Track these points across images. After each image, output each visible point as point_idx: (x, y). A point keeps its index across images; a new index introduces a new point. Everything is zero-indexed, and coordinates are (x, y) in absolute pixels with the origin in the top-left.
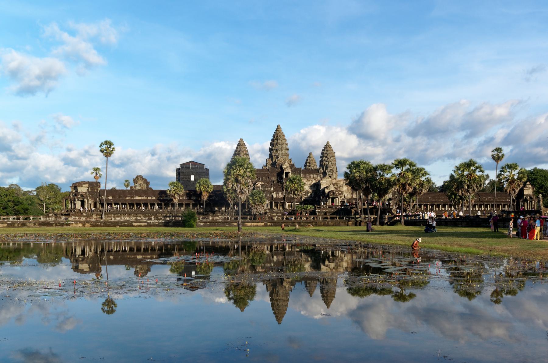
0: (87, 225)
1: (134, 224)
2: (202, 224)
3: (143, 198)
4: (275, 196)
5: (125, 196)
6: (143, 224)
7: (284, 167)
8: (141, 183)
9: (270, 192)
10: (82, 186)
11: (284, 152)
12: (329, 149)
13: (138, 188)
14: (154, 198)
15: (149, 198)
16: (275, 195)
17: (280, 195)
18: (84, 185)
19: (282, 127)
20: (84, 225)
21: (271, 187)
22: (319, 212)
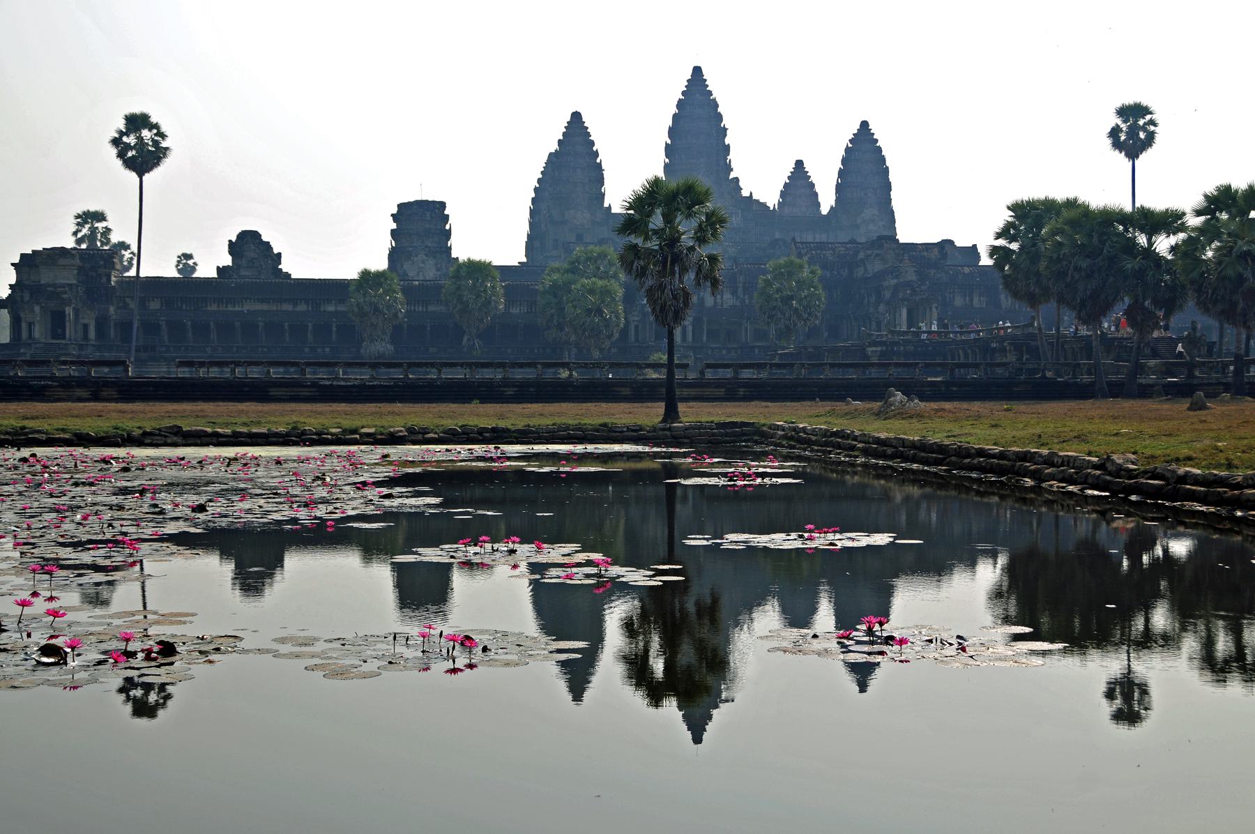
1: (274, 392)
3: (265, 307)
6: (305, 392)
8: (253, 255)
13: (243, 273)
14: (302, 307)
15: (287, 307)
18: (62, 261)
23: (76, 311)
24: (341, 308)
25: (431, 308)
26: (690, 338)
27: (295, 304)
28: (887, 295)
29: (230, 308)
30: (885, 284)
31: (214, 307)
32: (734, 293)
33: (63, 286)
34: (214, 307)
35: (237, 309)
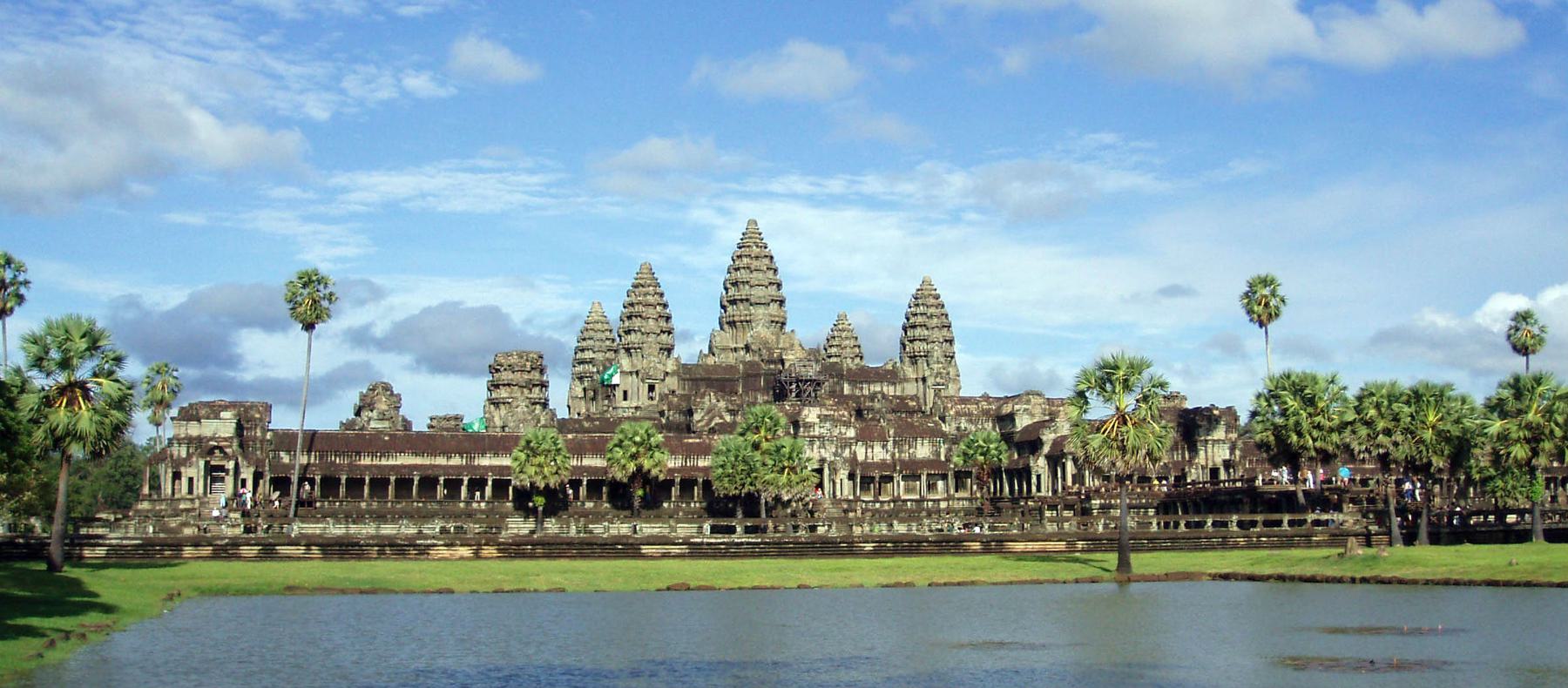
0: (489, 551)
1: (646, 549)
2: (869, 547)
3: (418, 461)
4: (861, 457)
5: (358, 453)
7: (790, 357)
8: (384, 407)
9: (845, 443)
10: (217, 417)
11: (774, 307)
12: (932, 301)
13: (373, 424)
14: (456, 461)
15: (441, 461)
16: (860, 452)
17: (879, 453)
18: (223, 414)
19: (762, 227)
20: (477, 556)
21: (847, 424)
22: (1102, 507)
23: (237, 465)
24: (497, 462)
25: (587, 462)
26: (846, 492)
27: (449, 458)
28: (1046, 449)
29: (384, 462)
30: (1044, 438)
31: (366, 461)
32: (884, 447)
33: (225, 439)
34: (366, 461)
35: (391, 462)
